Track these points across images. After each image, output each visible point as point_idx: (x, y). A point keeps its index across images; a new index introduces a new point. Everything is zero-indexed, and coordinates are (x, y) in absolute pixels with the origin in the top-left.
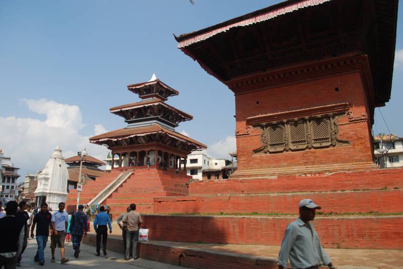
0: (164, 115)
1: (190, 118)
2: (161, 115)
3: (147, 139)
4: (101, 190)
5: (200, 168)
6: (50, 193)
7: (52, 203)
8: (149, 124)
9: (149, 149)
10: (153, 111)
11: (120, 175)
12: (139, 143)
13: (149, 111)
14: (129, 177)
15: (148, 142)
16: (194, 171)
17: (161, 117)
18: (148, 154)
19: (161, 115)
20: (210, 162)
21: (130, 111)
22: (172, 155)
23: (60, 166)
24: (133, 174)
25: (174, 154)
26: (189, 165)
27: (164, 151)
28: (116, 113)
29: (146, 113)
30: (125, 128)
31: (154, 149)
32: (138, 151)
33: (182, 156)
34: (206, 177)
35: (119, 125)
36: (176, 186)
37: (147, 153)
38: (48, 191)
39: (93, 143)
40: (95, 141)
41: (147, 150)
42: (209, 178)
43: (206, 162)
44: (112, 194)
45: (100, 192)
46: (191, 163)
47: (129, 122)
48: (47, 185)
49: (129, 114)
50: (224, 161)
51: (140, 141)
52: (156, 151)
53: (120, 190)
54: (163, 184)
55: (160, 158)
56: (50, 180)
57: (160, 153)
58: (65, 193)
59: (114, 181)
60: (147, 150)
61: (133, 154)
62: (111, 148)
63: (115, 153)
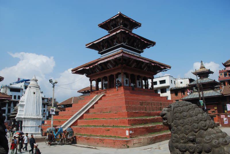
0: (128, 42)
1: (153, 44)
2: (126, 43)
4: (76, 112)
5: (168, 87)
6: (25, 118)
7: (27, 127)
8: (116, 52)
9: (116, 73)
11: (94, 98)
12: (109, 68)
13: (115, 41)
14: (101, 99)
15: (115, 66)
16: (163, 90)
17: (126, 44)
18: (117, 77)
19: (126, 43)
20: (176, 82)
21: (101, 44)
23: (34, 93)
24: (104, 96)
25: (141, 75)
26: (159, 85)
27: (130, 73)
29: (113, 44)
30: (99, 59)
31: (120, 71)
32: (108, 75)
33: (149, 77)
34: (174, 94)
35: (94, 56)
36: (141, 104)
38: (23, 117)
39: (74, 73)
40: (74, 72)
41: (114, 73)
42: (176, 94)
43: (173, 82)
44: (83, 115)
45: (75, 114)
46: (160, 84)
47: (102, 54)
48: (23, 111)
50: (188, 80)
51: (109, 67)
53: (92, 111)
54: (127, 102)
55: (128, 79)
56: (25, 106)
57: (127, 76)
58: (39, 117)
59: (88, 103)
61: (105, 79)
62: (89, 76)
63: (92, 79)
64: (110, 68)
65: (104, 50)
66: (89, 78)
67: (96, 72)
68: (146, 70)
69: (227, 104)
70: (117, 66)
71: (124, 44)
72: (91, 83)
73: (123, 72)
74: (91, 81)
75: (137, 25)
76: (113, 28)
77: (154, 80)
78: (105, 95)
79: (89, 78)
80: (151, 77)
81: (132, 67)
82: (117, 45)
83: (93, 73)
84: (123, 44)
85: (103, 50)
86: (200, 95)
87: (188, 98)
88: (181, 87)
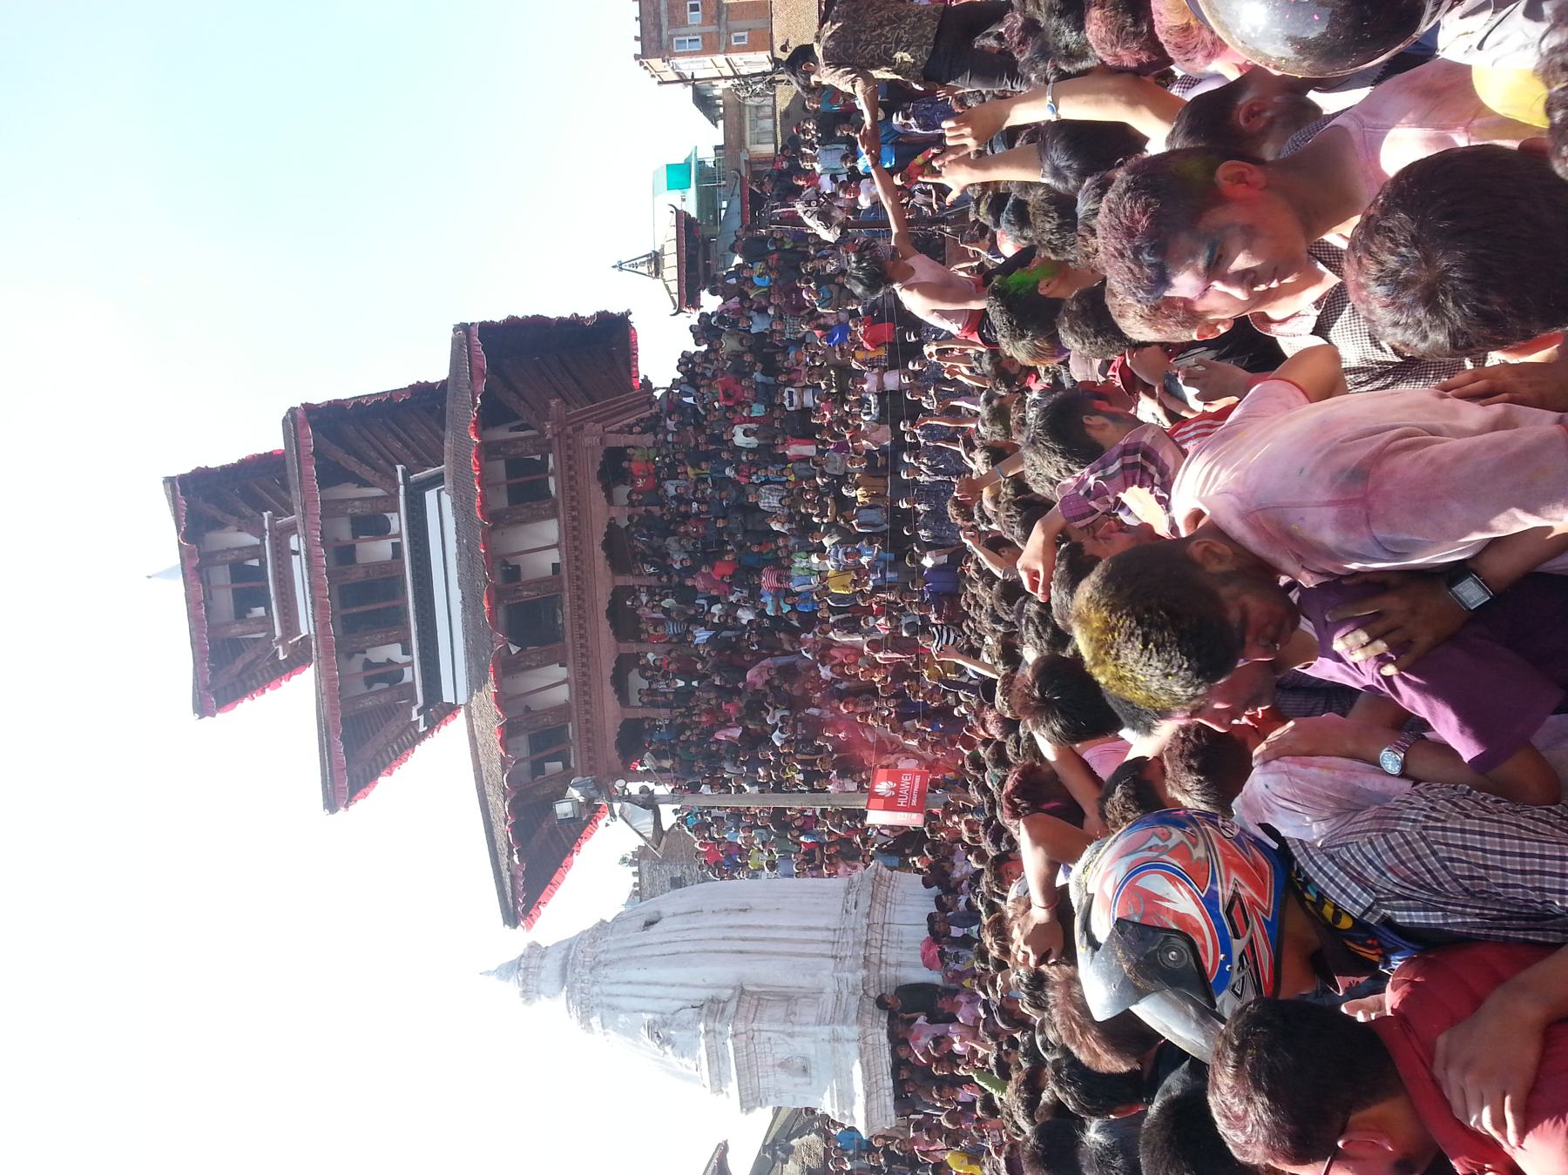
65: (410, 664)
67: (562, 711)
76: (260, 611)
82: (399, 535)
85: (407, 671)
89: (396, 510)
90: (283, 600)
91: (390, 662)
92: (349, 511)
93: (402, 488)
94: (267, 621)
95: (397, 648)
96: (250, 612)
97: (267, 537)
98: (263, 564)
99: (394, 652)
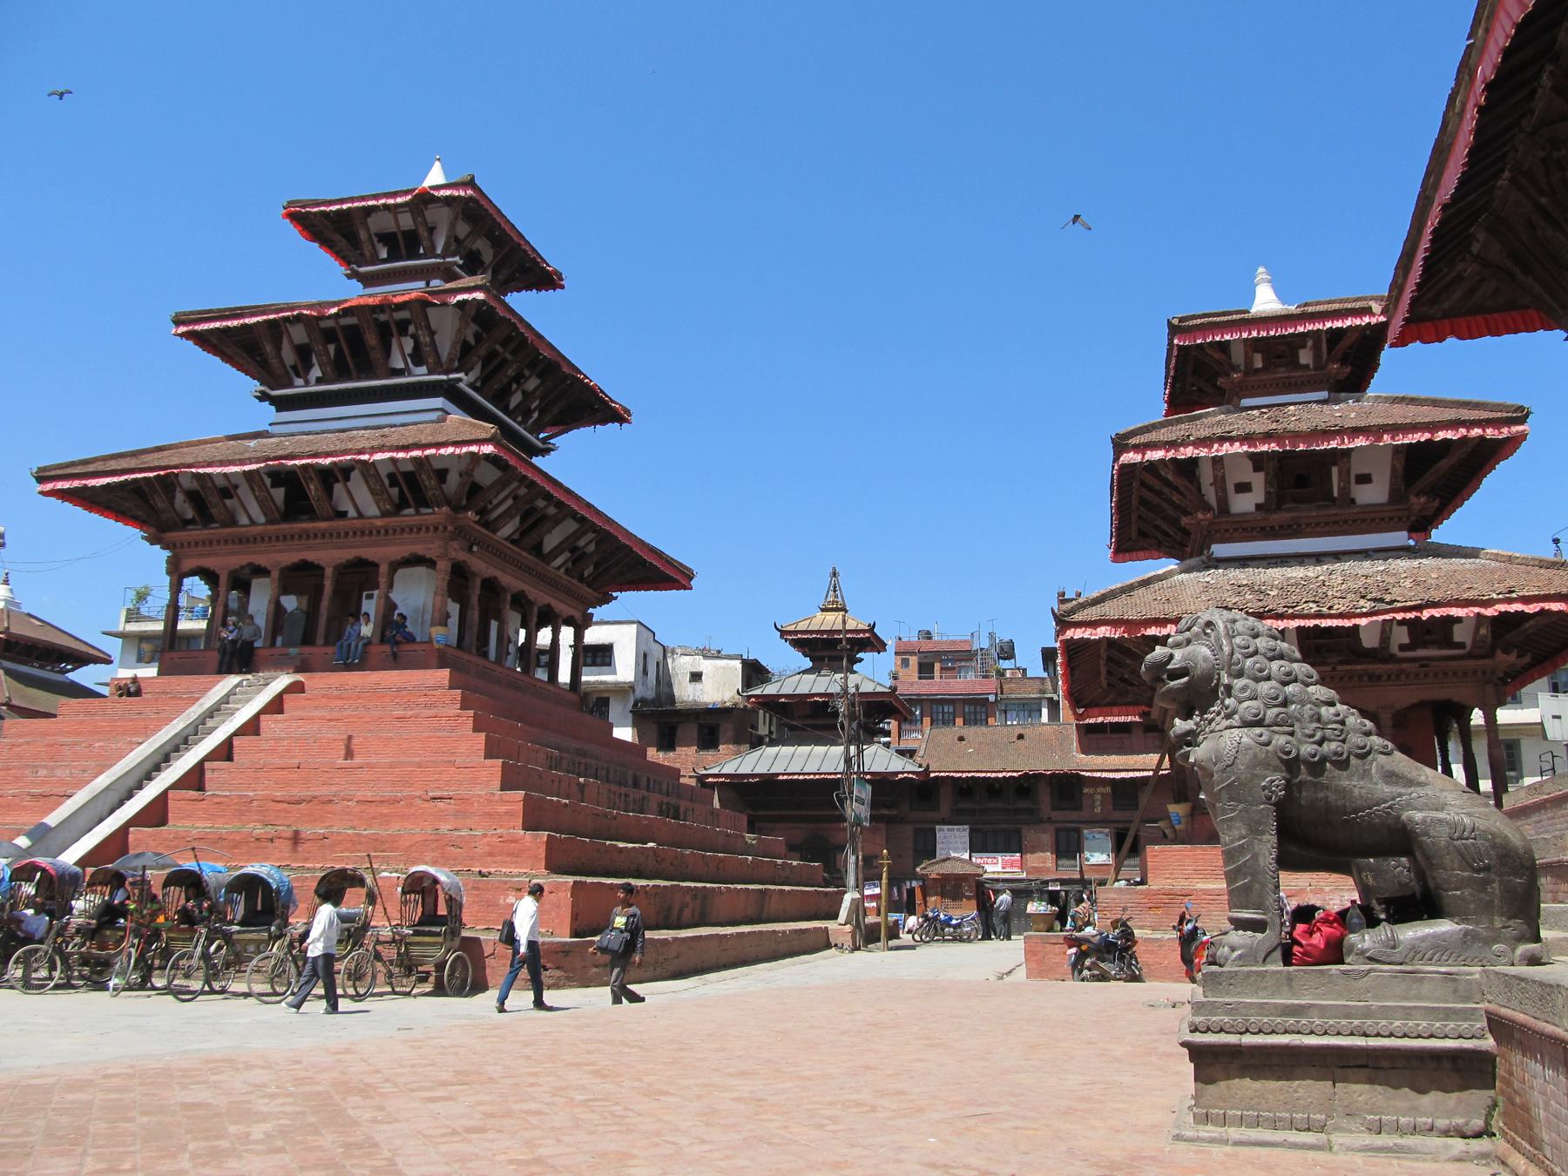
3: (395, 491)
5: (623, 690)
10: (433, 342)
12: (343, 515)
14: (276, 706)
16: (597, 704)
17: (471, 386)
19: (471, 377)
22: (520, 602)
24: (296, 688)
28: (201, 339)
29: (387, 352)
32: (328, 556)
37: (384, 569)
47: (282, 404)
49: (289, 356)
50: (738, 664)
52: (444, 566)
60: (380, 553)
64: (352, 513)
65: (307, 383)
66: (161, 555)
67: (232, 521)
68: (562, 570)
69: (937, 827)
70: (411, 511)
71: (464, 379)
72: (176, 588)
73: (453, 554)
74: (177, 573)
75: (546, 280)
76: (384, 254)
77: (593, 636)
78: (302, 684)
79: (167, 553)
80: (577, 615)
81: (499, 534)
82: (410, 374)
83: (204, 515)
84: (460, 380)
85: (299, 381)
86: (848, 761)
87: (740, 771)
88: (706, 704)
89: (430, 373)
90: (378, 276)
91: (309, 367)
92: (420, 332)
93: (444, 377)
94: (375, 260)
95: (320, 374)
96: (384, 246)
97: (438, 260)
98: (419, 257)
99: (316, 372)
